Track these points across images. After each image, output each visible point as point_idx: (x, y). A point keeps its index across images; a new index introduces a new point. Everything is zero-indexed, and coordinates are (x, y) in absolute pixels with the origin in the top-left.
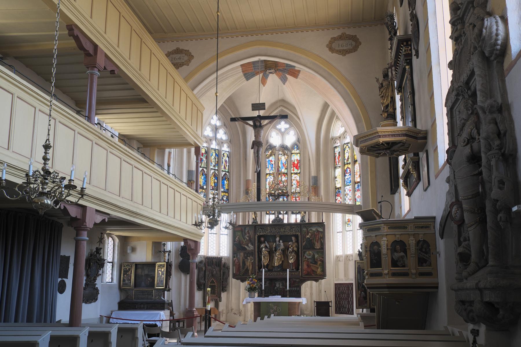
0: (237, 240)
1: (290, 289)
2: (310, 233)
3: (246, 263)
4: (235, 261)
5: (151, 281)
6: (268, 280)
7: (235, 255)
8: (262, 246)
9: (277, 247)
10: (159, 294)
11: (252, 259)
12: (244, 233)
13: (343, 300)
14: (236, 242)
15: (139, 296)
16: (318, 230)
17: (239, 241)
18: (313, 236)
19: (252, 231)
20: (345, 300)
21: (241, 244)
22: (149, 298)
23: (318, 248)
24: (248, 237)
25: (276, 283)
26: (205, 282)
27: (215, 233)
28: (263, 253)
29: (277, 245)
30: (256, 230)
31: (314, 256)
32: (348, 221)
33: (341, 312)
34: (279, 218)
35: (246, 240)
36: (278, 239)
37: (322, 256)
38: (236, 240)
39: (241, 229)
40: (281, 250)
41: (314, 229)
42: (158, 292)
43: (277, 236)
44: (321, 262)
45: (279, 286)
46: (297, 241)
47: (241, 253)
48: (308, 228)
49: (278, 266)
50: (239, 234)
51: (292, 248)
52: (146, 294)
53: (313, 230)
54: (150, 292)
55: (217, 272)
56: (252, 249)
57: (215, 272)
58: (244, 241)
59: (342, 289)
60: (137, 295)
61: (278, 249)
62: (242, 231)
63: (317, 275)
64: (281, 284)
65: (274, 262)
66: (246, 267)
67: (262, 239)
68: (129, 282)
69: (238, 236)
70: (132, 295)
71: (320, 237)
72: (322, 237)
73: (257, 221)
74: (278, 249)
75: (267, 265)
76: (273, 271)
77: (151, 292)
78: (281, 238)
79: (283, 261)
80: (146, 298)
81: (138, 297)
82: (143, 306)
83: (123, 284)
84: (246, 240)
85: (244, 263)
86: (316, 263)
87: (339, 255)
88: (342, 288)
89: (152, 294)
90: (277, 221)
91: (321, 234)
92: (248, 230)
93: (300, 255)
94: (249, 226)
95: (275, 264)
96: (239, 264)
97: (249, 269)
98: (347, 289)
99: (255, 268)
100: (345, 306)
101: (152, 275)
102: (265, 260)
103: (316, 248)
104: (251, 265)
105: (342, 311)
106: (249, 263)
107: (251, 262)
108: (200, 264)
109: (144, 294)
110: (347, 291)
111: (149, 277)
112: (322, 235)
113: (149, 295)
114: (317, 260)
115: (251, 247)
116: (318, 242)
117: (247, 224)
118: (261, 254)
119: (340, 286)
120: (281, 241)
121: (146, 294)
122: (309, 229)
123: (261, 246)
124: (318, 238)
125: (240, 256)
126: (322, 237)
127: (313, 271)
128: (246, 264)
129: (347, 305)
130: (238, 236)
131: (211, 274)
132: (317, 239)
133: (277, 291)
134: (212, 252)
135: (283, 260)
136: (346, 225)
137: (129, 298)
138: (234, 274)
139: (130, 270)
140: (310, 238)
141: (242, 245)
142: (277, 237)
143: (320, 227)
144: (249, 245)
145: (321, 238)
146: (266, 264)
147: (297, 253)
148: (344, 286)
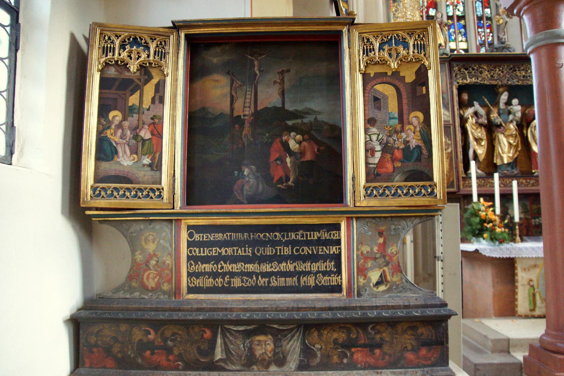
5: (309, 157)
8: (469, 112)
10: (383, 246)
15: (228, 267)
22: (311, 281)
30: (452, 72)
36: (504, 97)
42: (381, 234)
52: (287, 251)
54: (316, 235)
60: (217, 259)
68: (147, 160)
70: (169, 261)
77: (325, 235)
80: (291, 282)
81: (224, 275)
82: (270, 347)
83: (97, 179)
89: (333, 250)
99: (457, 167)
101: (308, 112)
109: (269, 251)
111: (290, 129)
113: (304, 259)
120: (515, 101)
121: (287, 251)
137: (151, 284)
139: (150, 78)
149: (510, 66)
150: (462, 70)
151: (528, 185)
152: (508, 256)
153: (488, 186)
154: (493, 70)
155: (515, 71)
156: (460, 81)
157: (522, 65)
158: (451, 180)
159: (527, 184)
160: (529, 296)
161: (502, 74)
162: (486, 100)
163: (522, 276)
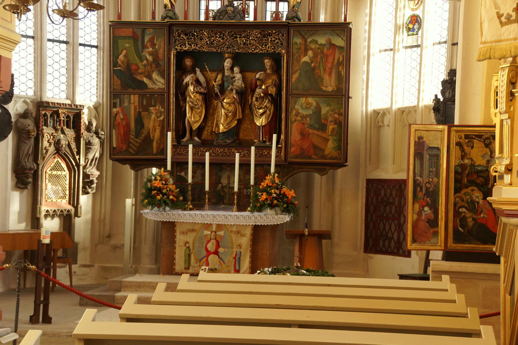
0: (123, 62)
2: (312, 50)
3: (145, 122)
4: (116, 115)
7: (118, 101)
8: (188, 79)
9: (226, 84)
11: (161, 113)
12: (140, 43)
13: (385, 221)
14: (120, 66)
16: (333, 42)
17: (128, 66)
18: (319, 57)
19: (163, 39)
20: (390, 221)
21: (133, 72)
23: (330, 89)
24: (150, 54)
25: (219, 174)
26: (38, 167)
27: (65, 40)
28: (190, 97)
29: (225, 79)
30: (172, 37)
31: (318, 110)
32: (411, 22)
33: (378, 249)
34: (232, 9)
35: (145, 62)
36: (227, 63)
37: (339, 111)
38: (120, 62)
39: (134, 32)
40: (237, 91)
41: (322, 40)
43: (226, 55)
44: (335, 126)
46: (277, 68)
47: (132, 96)
48: (306, 38)
49: (227, 131)
50: (127, 45)
51: (263, 87)
53: (319, 42)
55: (69, 142)
56: (160, 87)
57: (64, 142)
58: (140, 64)
59: (385, 195)
61: (229, 89)
62: (134, 37)
63: (324, 157)
65: (217, 121)
66: (145, 132)
67: (188, 62)
69: (124, 52)
71: (336, 61)
72: (341, 59)
73: (175, 14)
74: (229, 89)
75: (201, 129)
76: (213, 144)
78: (237, 59)
79: (239, 120)
84: (145, 62)
85: (140, 122)
86: (323, 127)
87: (381, 110)
88: (385, 191)
90: (226, 16)
91: (340, 54)
92: (150, 36)
93: (284, 105)
94: (153, 25)
95: (219, 127)
96: (128, 125)
97: (154, 136)
98: (396, 195)
100: (390, 235)
102: (194, 117)
103: (324, 89)
104: (157, 127)
105: (381, 247)
106: (152, 122)
107: (159, 120)
108: (22, 120)
110: (397, 199)
112: (341, 56)
114: (326, 120)
115: (160, 82)
116: (330, 74)
117: (148, 19)
118: (185, 101)
119: (380, 187)
120: (236, 69)
122: (309, 40)
123: (183, 80)
124: (333, 63)
125: (130, 102)
126: (343, 61)
127: (315, 147)
128: (146, 126)
129: (396, 234)
130: (124, 52)
131: (52, 146)
132: (329, 65)
134: (56, 91)
135: (241, 117)
136: (405, 33)
138: (114, 148)
140: (312, 62)
141: (134, 76)
142: (226, 58)
143: (338, 35)
144: (155, 76)
145: (339, 63)
146: (195, 126)
147: (276, 101)
148: (391, 187)
149: (231, 32)
150: (182, 36)
152: (168, 220)
153: (199, 154)
154: (213, 36)
155: (237, 37)
156: (179, 48)
157: (244, 31)
158: (161, 147)
160: (185, 256)
161: (221, 41)
162: (206, 67)
163: (180, 239)
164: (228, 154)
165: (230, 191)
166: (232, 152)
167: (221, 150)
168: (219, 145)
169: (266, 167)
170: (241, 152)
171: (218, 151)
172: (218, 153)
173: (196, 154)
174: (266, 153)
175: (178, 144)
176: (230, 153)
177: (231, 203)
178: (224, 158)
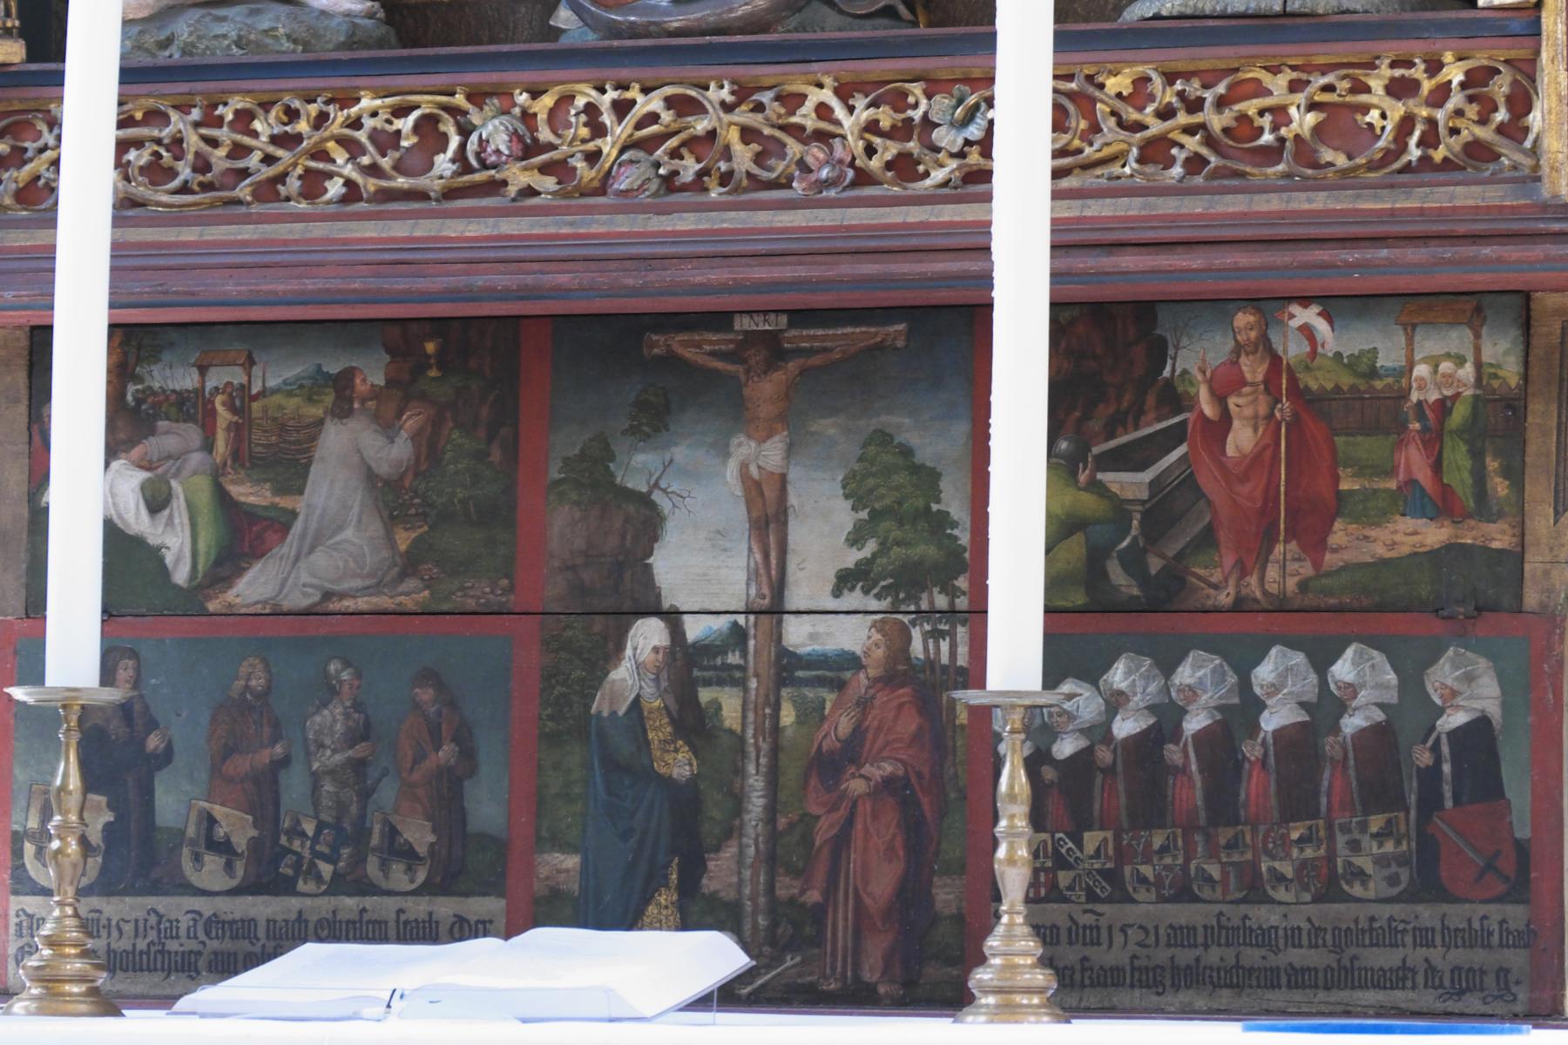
1: (1167, 716)
6: (373, 372)
45: (774, 609)
64: (844, 516)
133: (679, 764)
151: (905, 167)
153: (335, 188)
159: (889, 150)
164: (743, 157)
165: (788, 716)
166: (797, 131)
167: (647, 104)
168: (615, 31)
169: (1307, 331)
170: (928, 124)
171: (599, 130)
172: (593, 157)
173: (294, 184)
174: (1303, 121)
175: (32, 57)
176: (767, 151)
177: (814, 896)
178: (686, 222)
